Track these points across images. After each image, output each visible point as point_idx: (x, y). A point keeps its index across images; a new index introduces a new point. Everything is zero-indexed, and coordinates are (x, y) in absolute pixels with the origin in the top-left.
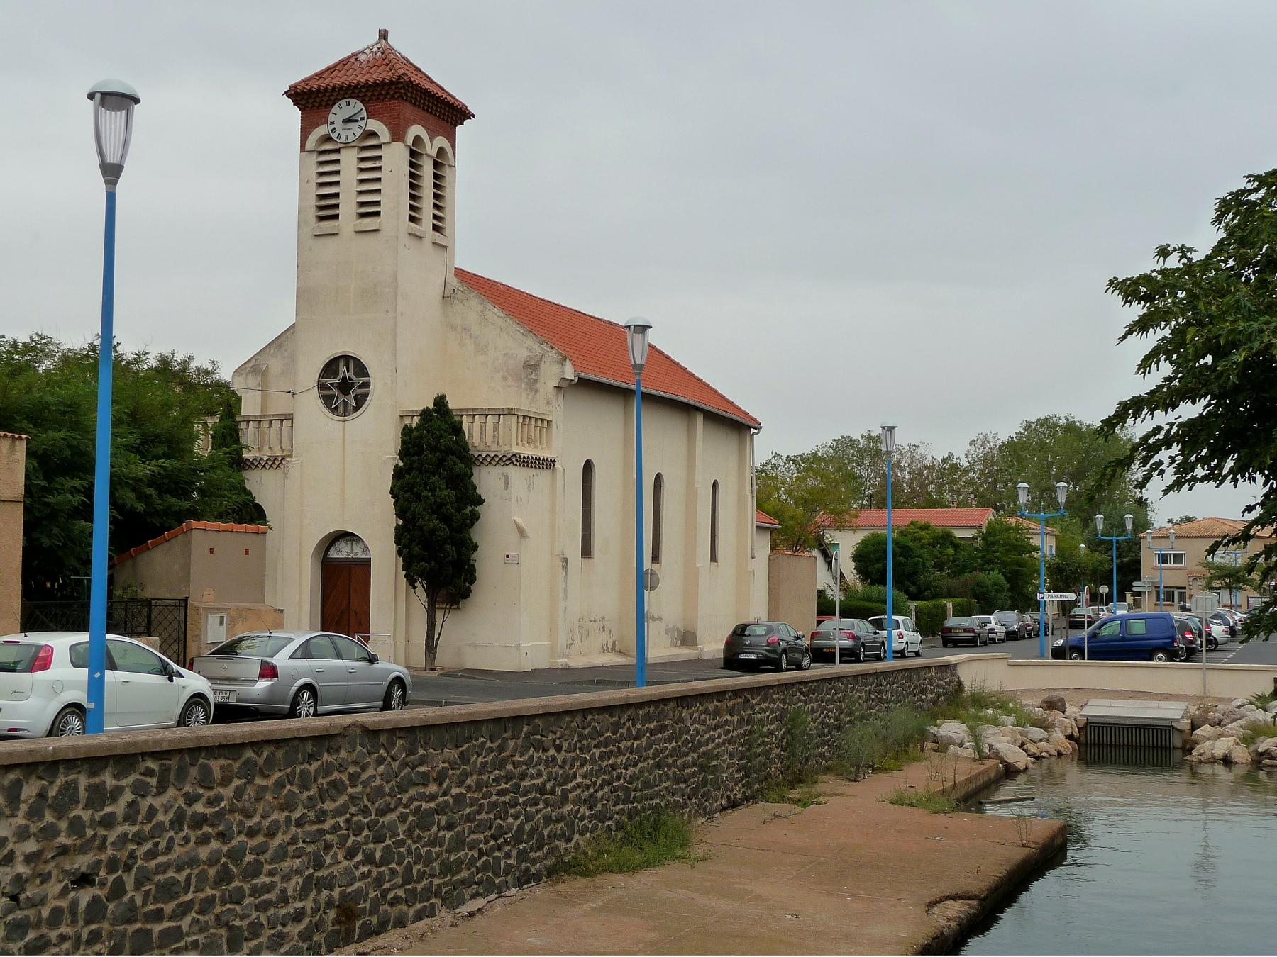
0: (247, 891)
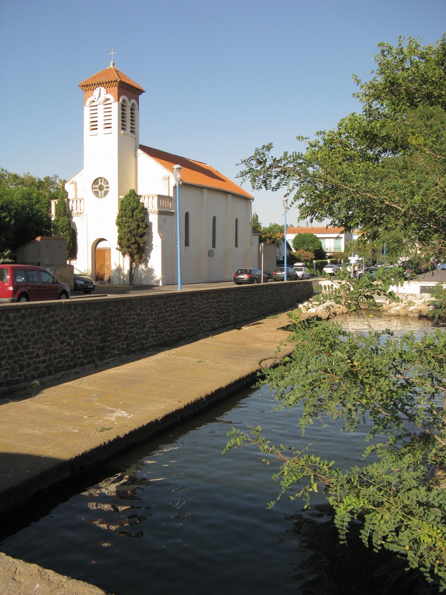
0: (25, 354)
